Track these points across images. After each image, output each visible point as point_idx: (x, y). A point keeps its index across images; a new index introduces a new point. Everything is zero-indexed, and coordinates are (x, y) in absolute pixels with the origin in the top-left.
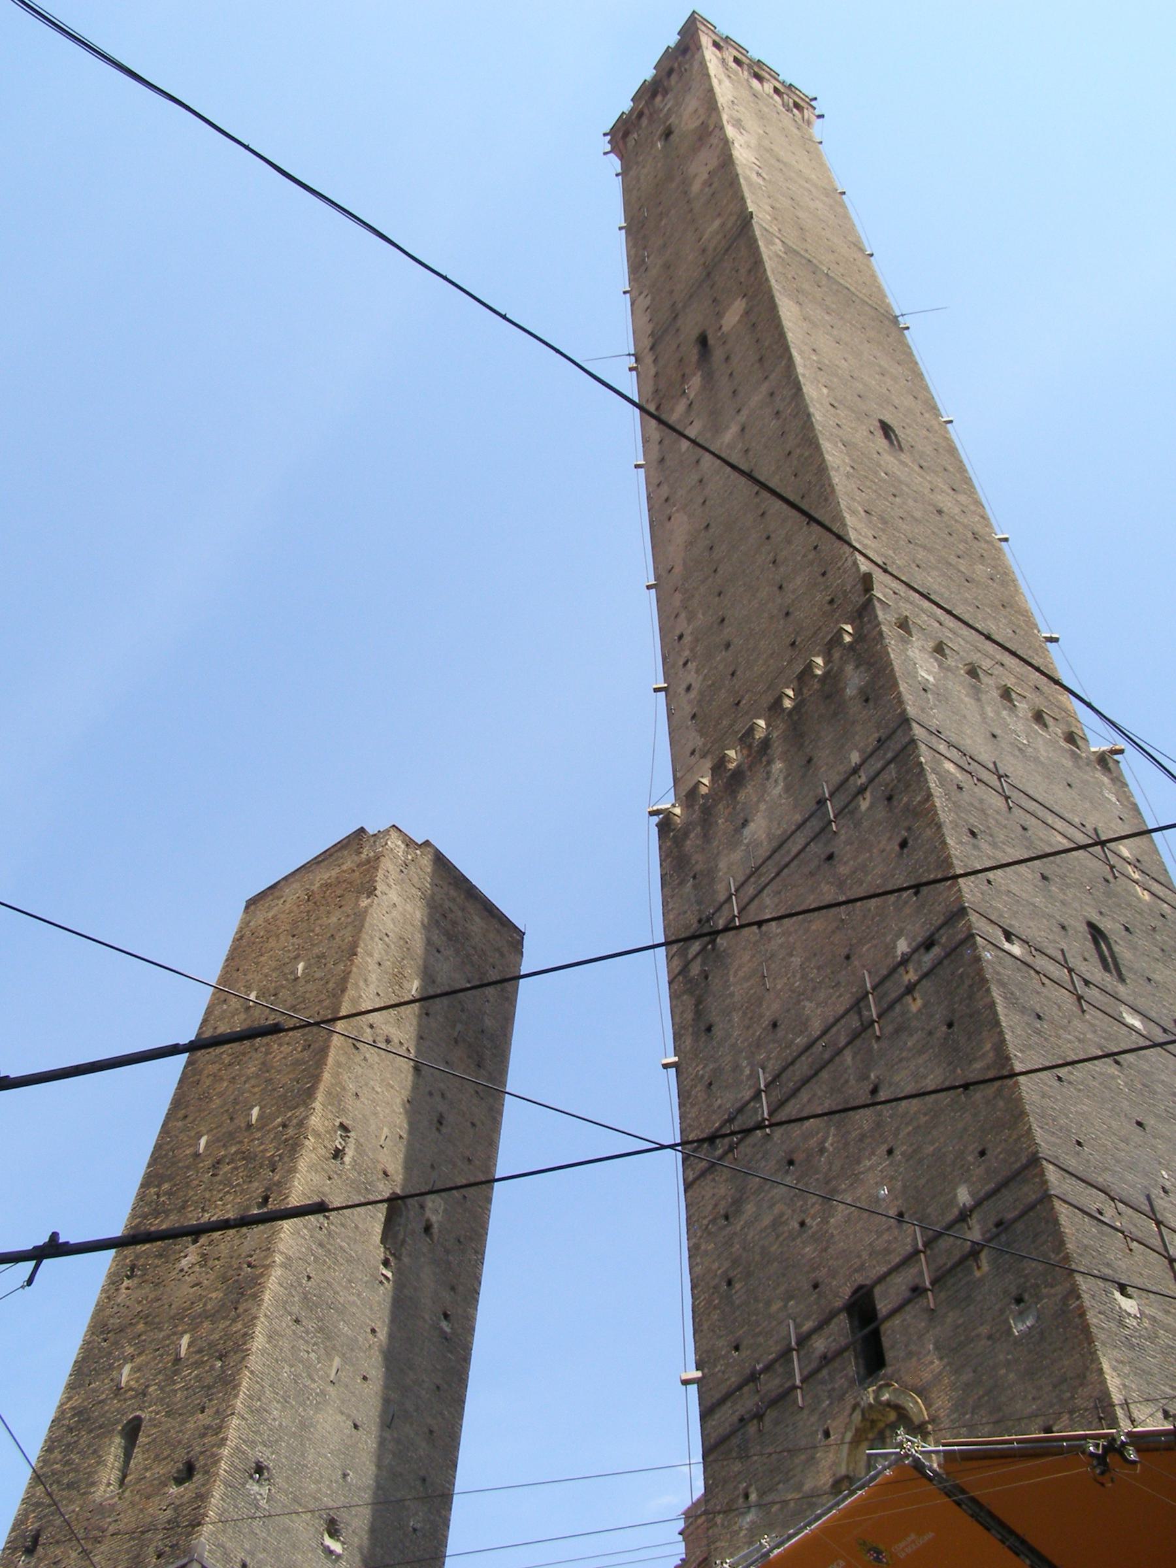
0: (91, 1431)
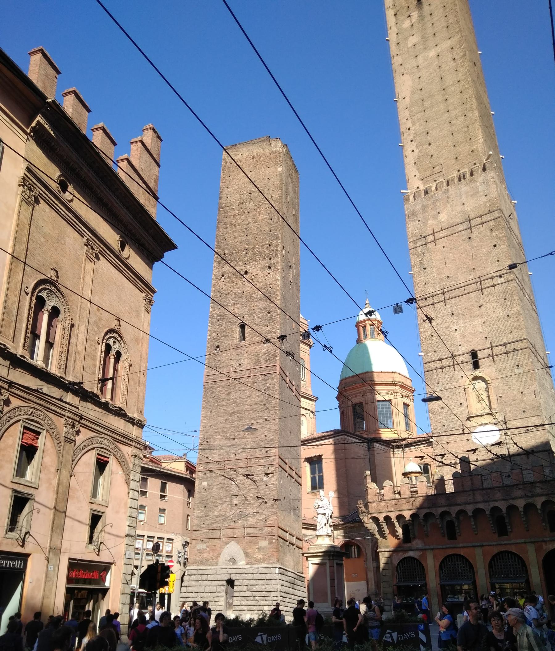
0: (226, 322)
